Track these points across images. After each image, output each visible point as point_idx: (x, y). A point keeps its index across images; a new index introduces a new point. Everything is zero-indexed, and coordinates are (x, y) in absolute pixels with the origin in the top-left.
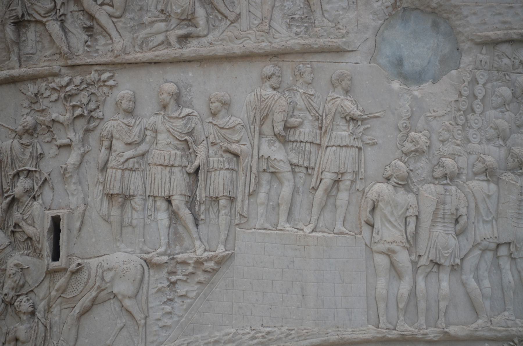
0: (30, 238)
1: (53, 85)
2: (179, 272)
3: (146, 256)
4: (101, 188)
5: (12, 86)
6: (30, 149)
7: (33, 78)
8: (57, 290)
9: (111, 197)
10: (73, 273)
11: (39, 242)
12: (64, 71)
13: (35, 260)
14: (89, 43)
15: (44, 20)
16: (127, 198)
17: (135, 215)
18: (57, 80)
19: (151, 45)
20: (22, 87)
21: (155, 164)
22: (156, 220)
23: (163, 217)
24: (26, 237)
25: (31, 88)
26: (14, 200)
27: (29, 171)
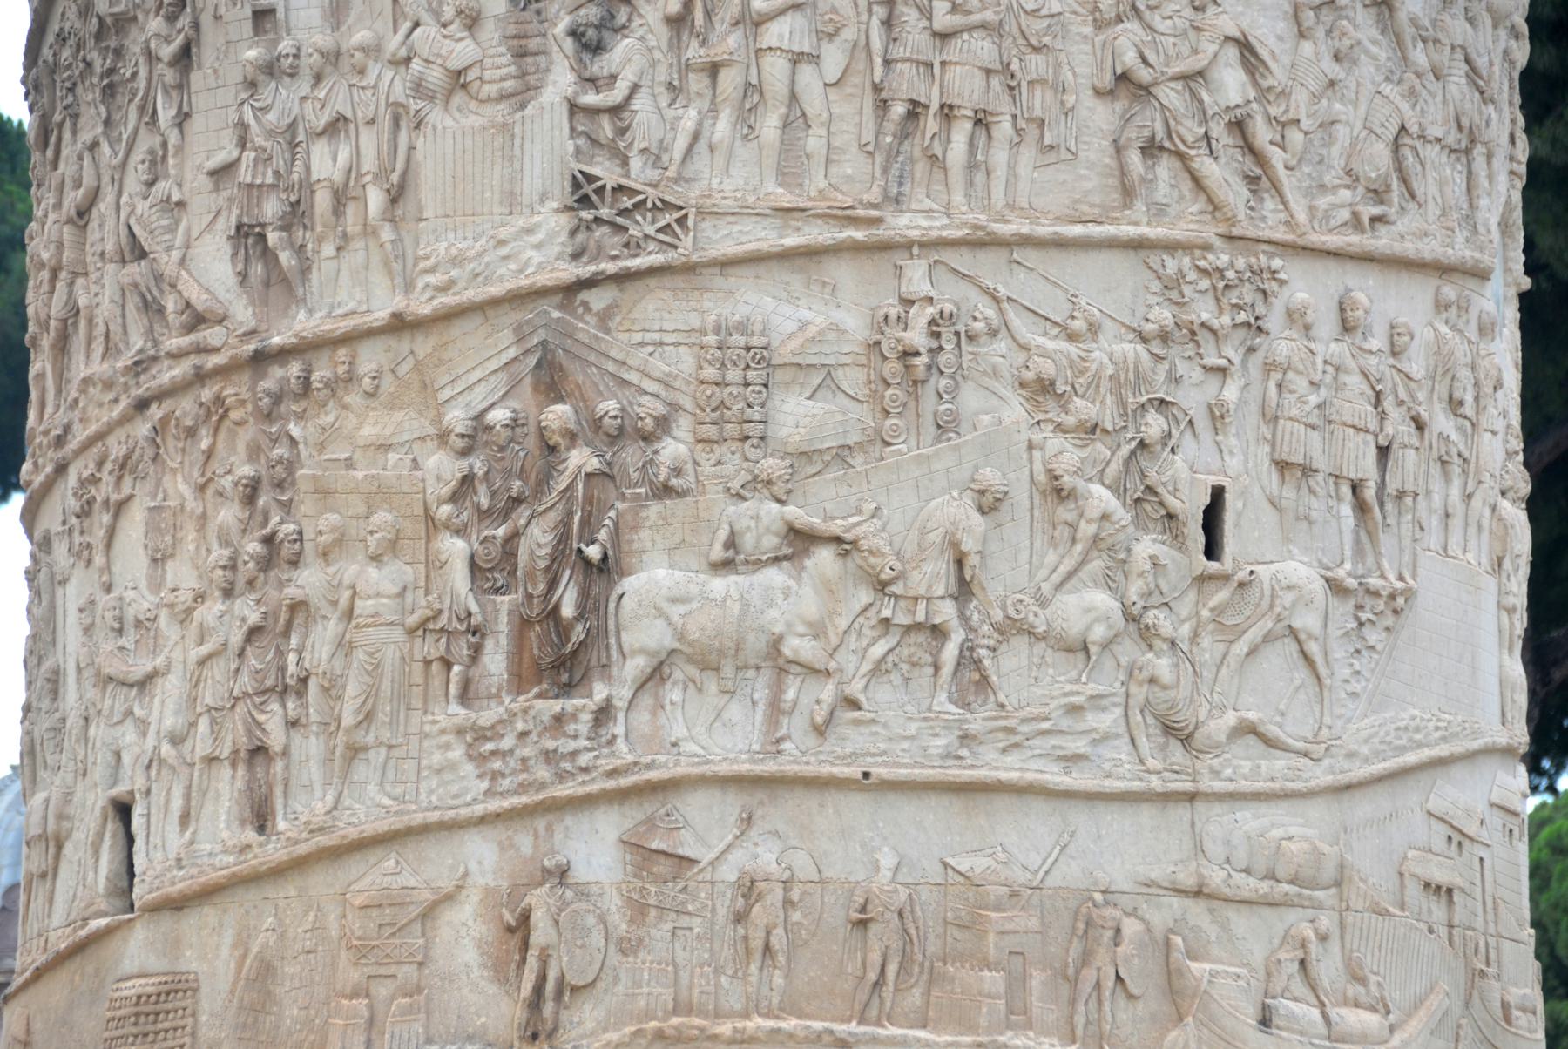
0: (1170, 516)
1: (1202, 263)
2: (1368, 607)
3: (1329, 574)
4: (1267, 449)
5: (1132, 253)
6: (1166, 365)
7: (1172, 247)
8: (1212, 610)
9: (1283, 466)
10: (1241, 585)
11: (1184, 524)
12: (1217, 242)
13: (1174, 553)
14: (1252, 203)
15: (1193, 152)
16: (1307, 471)
17: (1315, 503)
18: (1210, 257)
19: (1333, 223)
20: (1154, 260)
21: (1345, 424)
22: (1338, 517)
23: (1346, 510)
24: (1163, 512)
25: (1171, 265)
26: (1142, 445)
27: (1162, 401)
